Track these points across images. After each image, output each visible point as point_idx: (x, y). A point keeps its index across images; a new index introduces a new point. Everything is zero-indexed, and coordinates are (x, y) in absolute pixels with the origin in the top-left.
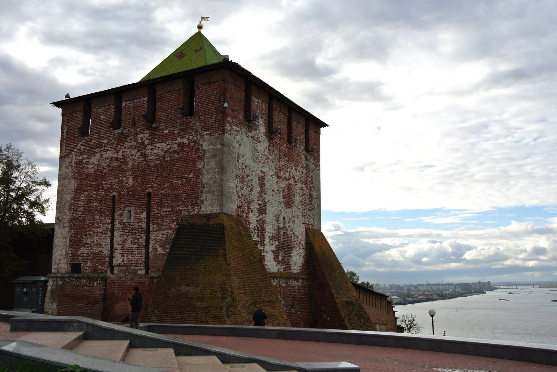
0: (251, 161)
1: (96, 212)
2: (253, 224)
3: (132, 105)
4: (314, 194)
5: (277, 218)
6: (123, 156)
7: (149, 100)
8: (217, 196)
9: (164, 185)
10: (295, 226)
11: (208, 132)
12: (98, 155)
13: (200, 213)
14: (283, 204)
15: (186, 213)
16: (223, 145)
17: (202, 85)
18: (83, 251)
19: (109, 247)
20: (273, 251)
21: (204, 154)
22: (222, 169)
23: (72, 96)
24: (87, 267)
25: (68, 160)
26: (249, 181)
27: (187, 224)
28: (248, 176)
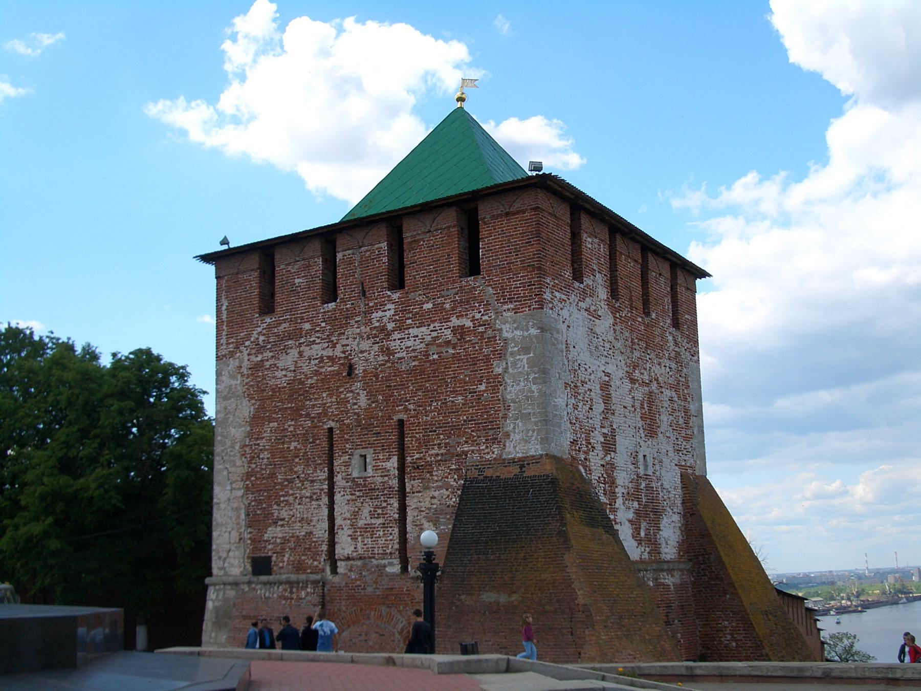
0: (587, 354)
1: (297, 460)
2: (596, 474)
3: (357, 257)
4: (692, 407)
5: (634, 456)
6: (344, 352)
7: (390, 246)
8: (536, 423)
9: (430, 405)
10: (663, 471)
11: (511, 306)
12: (294, 353)
13: (504, 456)
14: (641, 431)
15: (476, 456)
16: (542, 329)
17: (493, 217)
18: (274, 533)
19: (325, 525)
20: (630, 521)
21: (505, 347)
22: (543, 374)
23: (233, 245)
24: (283, 563)
25: (233, 364)
26: (586, 392)
27: (482, 477)
28: (583, 383)
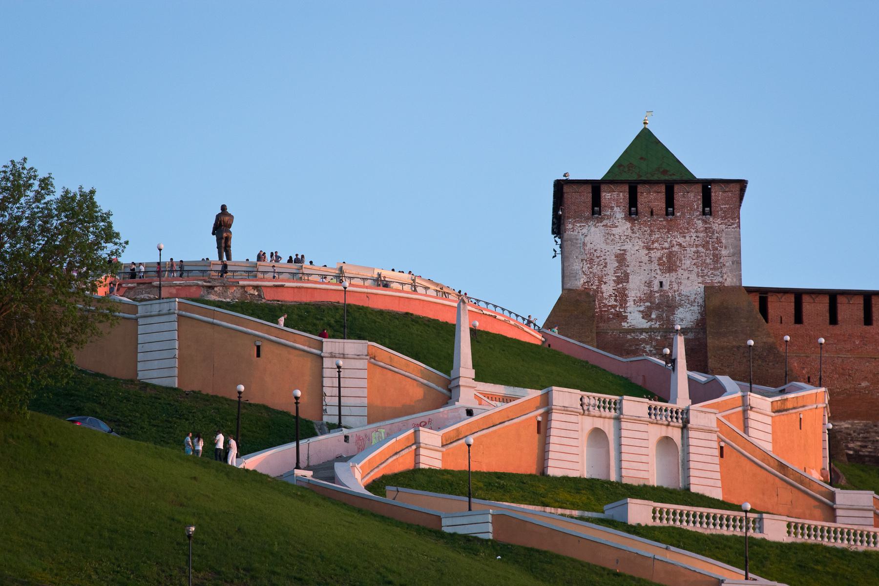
10: (682, 287)
14: (658, 272)
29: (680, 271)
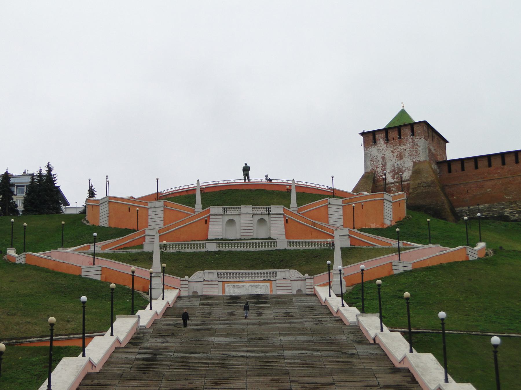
29: (404, 159)
